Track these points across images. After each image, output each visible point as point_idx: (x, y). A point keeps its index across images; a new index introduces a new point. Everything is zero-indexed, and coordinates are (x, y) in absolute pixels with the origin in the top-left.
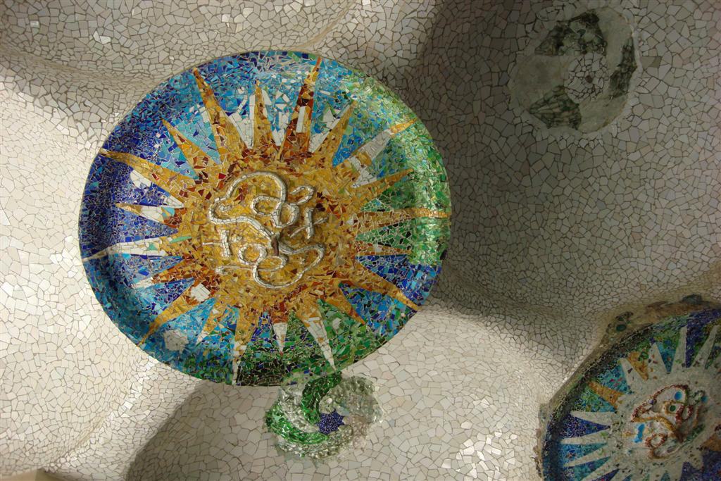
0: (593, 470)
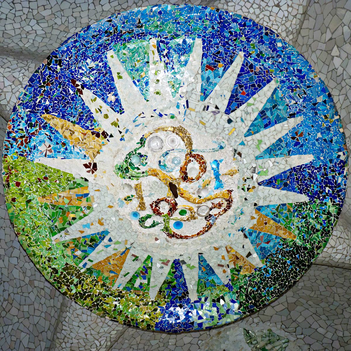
0: (262, 113)
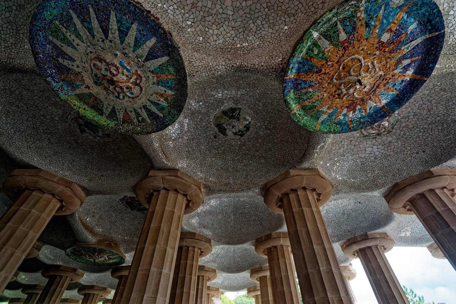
0: (119, 30)
